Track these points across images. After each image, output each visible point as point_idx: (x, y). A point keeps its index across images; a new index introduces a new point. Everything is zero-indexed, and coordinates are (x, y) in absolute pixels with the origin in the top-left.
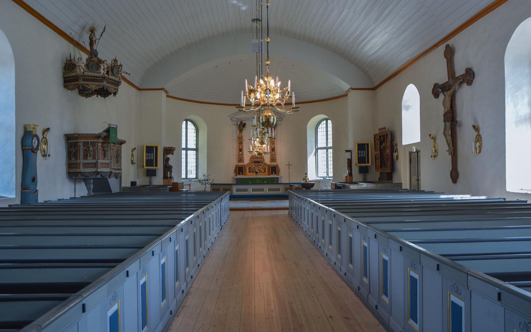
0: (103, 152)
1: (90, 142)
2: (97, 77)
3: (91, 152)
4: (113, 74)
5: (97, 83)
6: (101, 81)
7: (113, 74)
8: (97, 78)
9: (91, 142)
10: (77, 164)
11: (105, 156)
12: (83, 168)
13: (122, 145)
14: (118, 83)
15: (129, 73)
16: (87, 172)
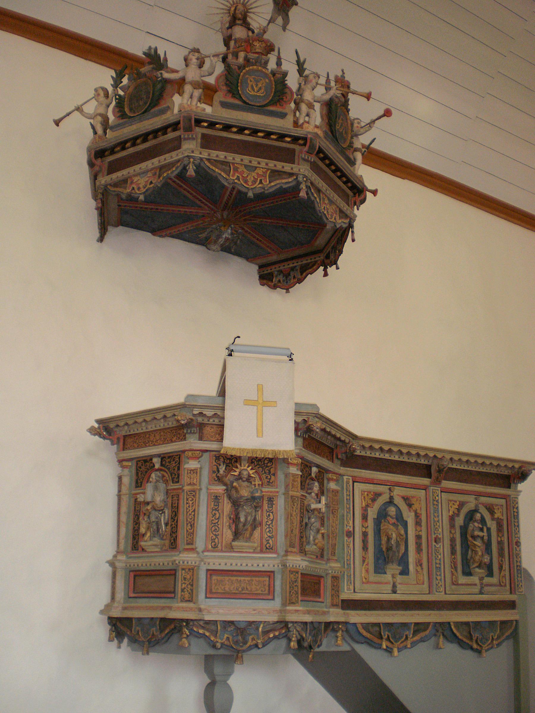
0: (227, 507)
1: (157, 462)
2: (155, 133)
3: (154, 508)
4: (241, 99)
5: (156, 162)
6: (176, 144)
7: (241, 99)
9: (163, 457)
10: (172, 573)
11: (237, 535)
12: (174, 598)
13: (521, 486)
14: (297, 148)
15: (366, 91)
16: (139, 619)
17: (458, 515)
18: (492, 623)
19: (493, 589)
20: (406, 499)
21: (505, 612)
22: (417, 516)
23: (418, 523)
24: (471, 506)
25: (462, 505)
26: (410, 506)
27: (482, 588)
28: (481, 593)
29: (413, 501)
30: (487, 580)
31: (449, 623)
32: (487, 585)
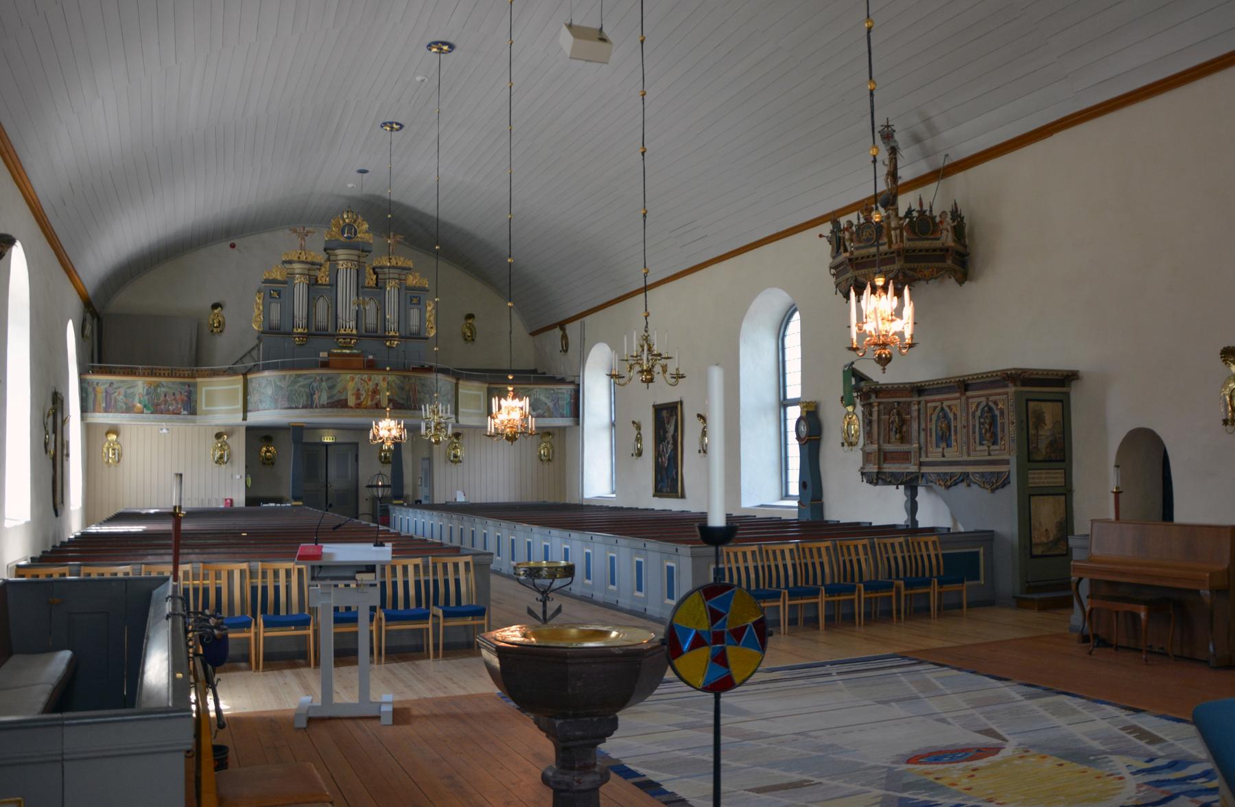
8: (863, 260)
17: (977, 410)
18: (992, 473)
19: (997, 452)
20: (949, 407)
21: (983, 467)
22: (955, 415)
23: (955, 419)
24: (984, 403)
25: (979, 404)
26: (951, 410)
27: (989, 452)
28: (989, 455)
29: (952, 407)
30: (993, 447)
31: (968, 473)
32: (992, 450)
